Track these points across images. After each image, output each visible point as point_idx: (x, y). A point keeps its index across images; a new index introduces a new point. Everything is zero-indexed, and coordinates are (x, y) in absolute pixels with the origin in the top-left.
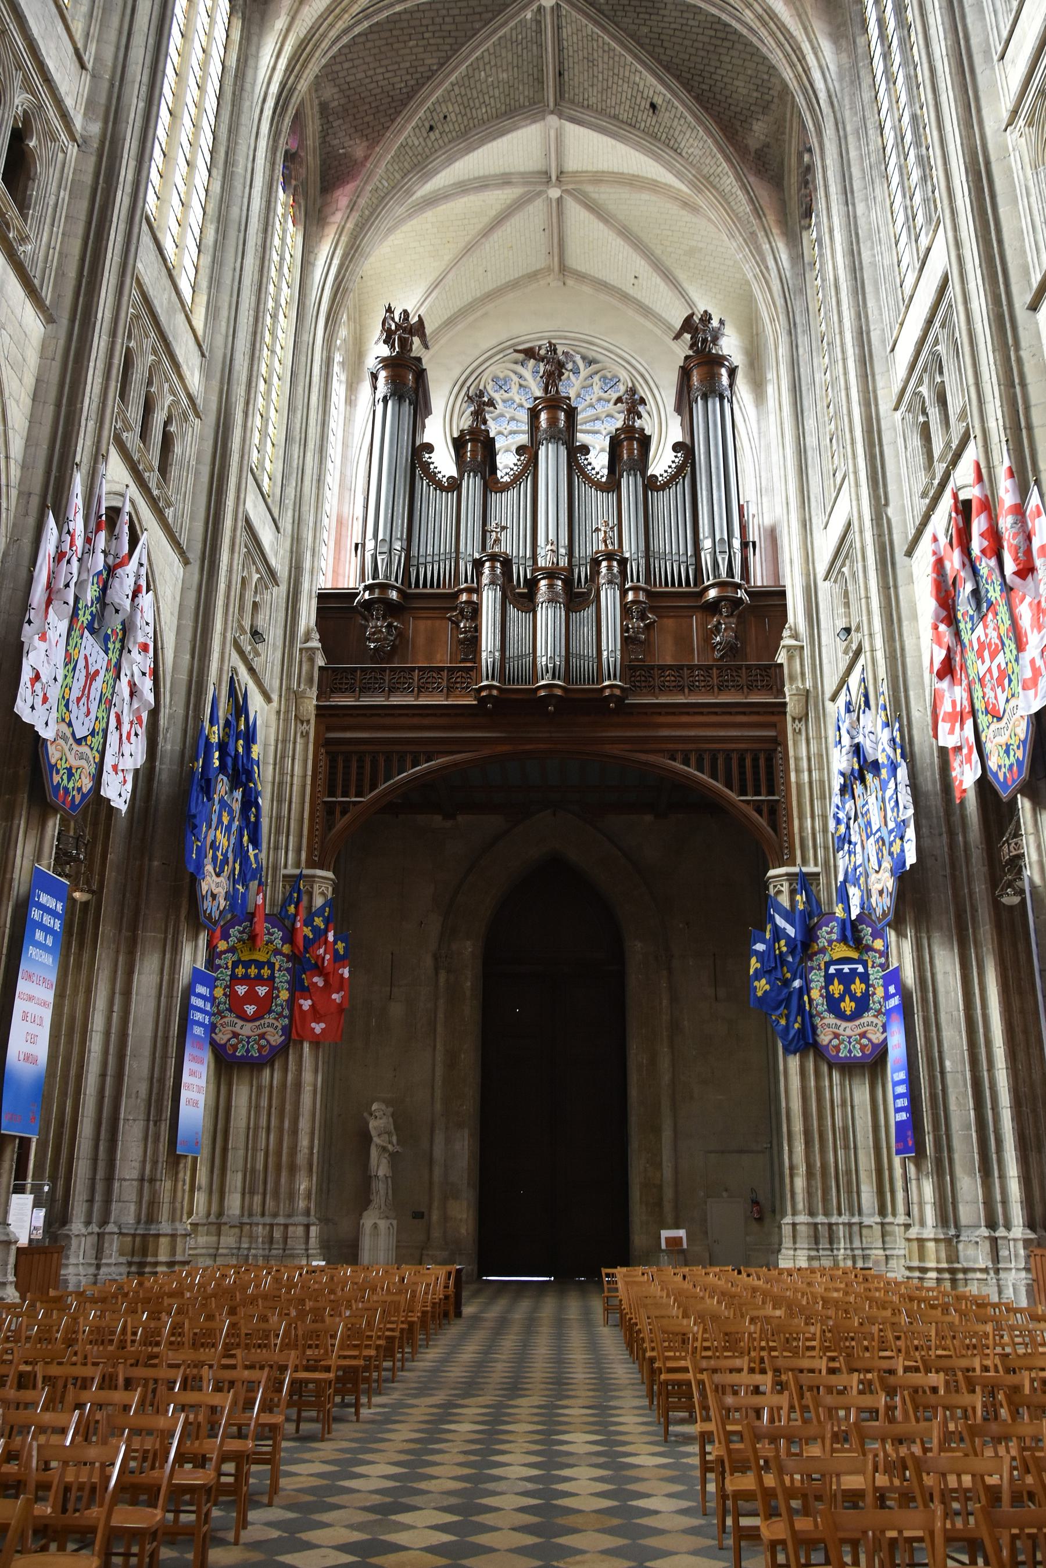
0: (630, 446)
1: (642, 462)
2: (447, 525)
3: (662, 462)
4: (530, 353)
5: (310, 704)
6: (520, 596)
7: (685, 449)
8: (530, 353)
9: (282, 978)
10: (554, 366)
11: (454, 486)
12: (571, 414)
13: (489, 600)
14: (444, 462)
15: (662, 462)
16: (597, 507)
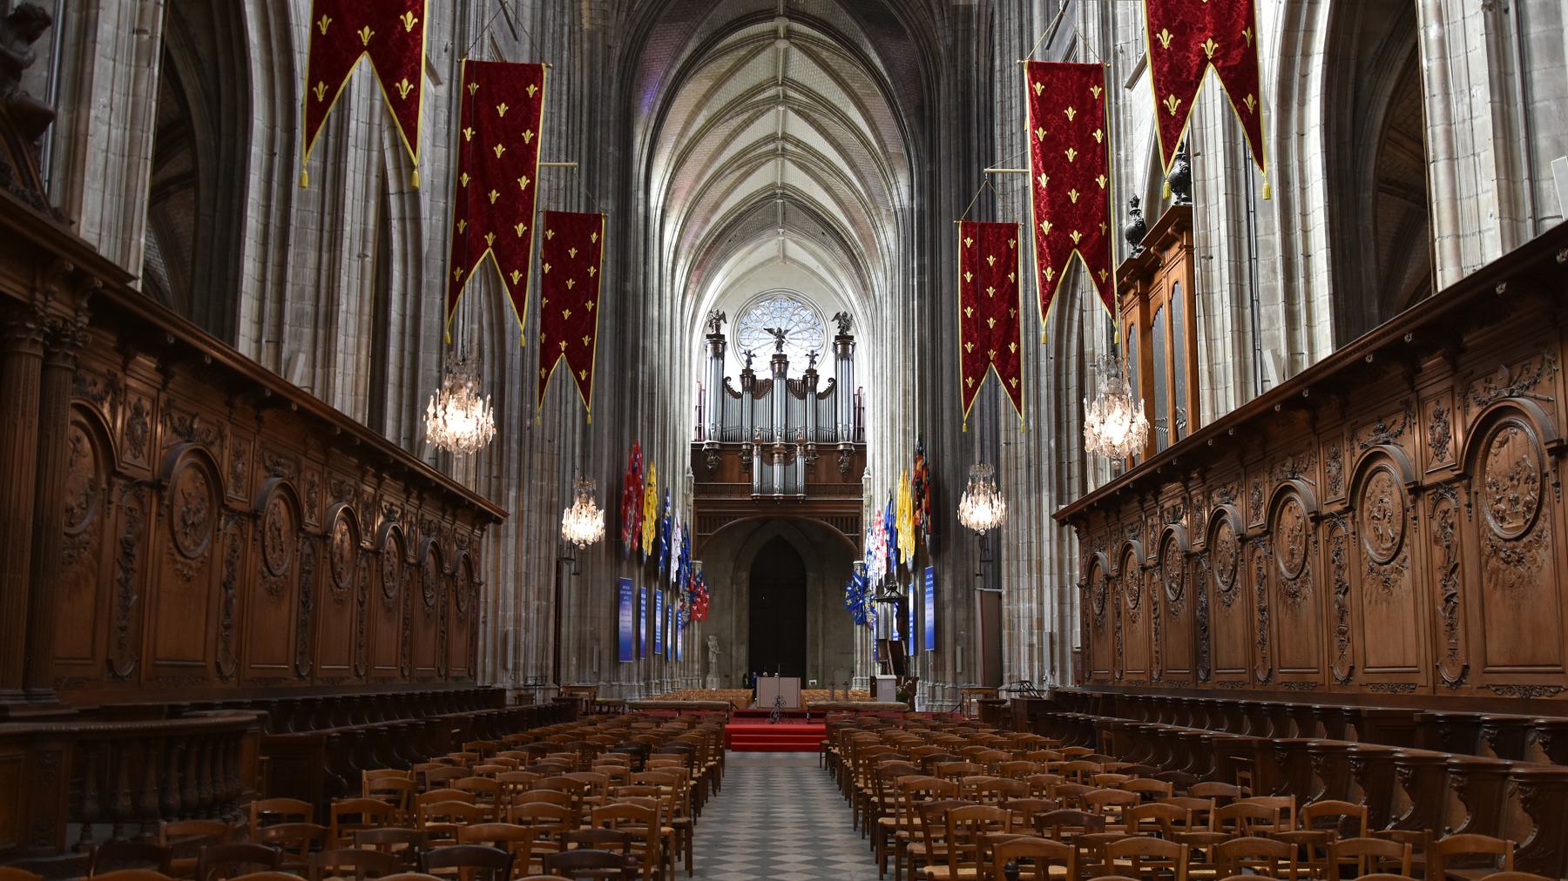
0: (812, 374)
1: (814, 388)
2: (737, 414)
3: (822, 386)
4: (770, 331)
5: (691, 499)
6: (767, 453)
7: (833, 381)
8: (770, 331)
9: (687, 599)
10: (780, 336)
11: (737, 396)
12: (787, 363)
13: (756, 461)
14: (737, 386)
15: (822, 386)
16: (797, 403)
